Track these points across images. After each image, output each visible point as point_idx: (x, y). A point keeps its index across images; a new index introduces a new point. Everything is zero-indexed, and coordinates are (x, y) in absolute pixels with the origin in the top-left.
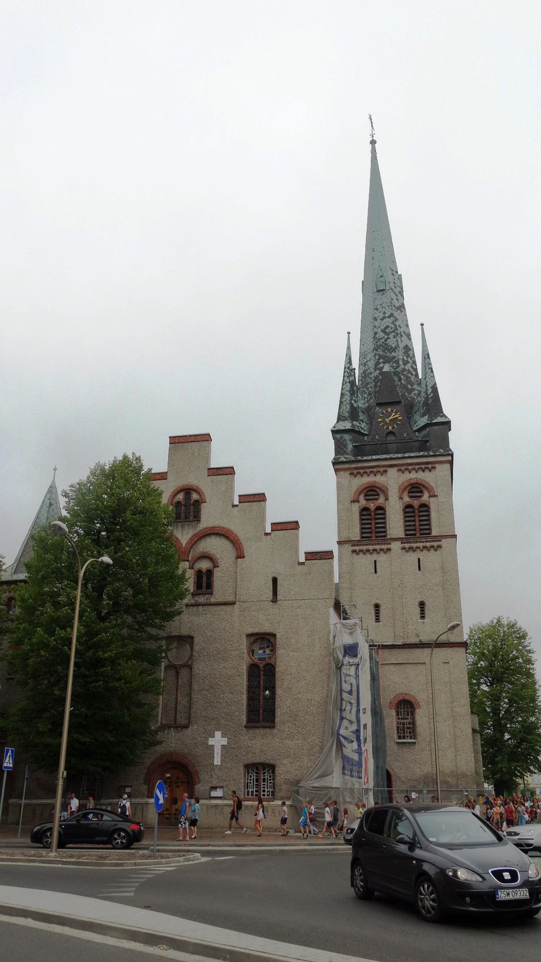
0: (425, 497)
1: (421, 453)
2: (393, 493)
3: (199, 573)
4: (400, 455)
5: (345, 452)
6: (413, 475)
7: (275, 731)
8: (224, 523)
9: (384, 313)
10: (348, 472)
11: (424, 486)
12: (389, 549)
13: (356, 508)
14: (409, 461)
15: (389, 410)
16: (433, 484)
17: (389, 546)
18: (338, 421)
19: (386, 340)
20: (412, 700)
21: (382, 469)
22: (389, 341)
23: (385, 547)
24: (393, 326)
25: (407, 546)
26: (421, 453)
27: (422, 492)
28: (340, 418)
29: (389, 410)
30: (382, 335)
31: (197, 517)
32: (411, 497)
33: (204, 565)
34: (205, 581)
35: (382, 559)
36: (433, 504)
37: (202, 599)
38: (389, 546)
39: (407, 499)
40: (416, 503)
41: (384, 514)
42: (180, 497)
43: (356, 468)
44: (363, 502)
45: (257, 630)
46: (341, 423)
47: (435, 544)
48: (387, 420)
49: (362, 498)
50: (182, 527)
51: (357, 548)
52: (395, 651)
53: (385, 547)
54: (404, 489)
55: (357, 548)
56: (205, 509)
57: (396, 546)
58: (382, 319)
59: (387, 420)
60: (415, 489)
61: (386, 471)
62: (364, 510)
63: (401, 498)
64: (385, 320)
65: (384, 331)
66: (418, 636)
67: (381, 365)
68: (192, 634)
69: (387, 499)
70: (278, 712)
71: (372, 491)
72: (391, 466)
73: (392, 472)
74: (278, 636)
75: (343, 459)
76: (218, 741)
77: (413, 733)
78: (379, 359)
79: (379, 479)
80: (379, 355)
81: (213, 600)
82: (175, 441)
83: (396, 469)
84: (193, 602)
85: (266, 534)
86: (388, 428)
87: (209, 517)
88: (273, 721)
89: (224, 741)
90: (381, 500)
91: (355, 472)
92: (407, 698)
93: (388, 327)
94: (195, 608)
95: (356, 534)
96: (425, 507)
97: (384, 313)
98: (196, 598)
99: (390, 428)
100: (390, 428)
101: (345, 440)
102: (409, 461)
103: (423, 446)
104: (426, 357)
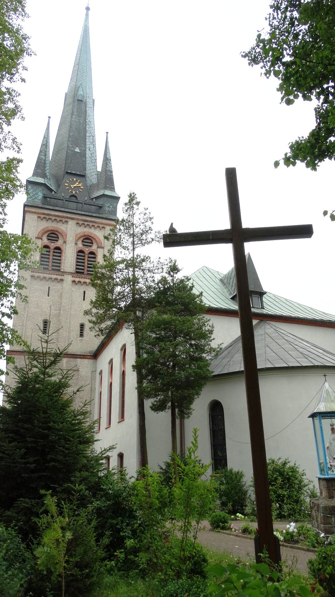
0: (94, 248)
11: (95, 239)
12: (62, 280)
15: (75, 179)
17: (62, 277)
18: (33, 176)
21: (64, 220)
23: (59, 277)
25: (77, 280)
29: (75, 179)
32: (84, 245)
35: (56, 287)
38: (62, 277)
39: (80, 245)
40: (87, 250)
41: (61, 253)
48: (72, 186)
51: (36, 275)
53: (59, 277)
54: (79, 238)
57: (69, 279)
59: (72, 186)
60: (88, 240)
63: (76, 244)
69: (65, 242)
71: (53, 235)
72: (73, 219)
73: (72, 223)
79: (61, 227)
83: (76, 222)
90: (59, 243)
91: (42, 216)
99: (74, 192)
100: (74, 192)
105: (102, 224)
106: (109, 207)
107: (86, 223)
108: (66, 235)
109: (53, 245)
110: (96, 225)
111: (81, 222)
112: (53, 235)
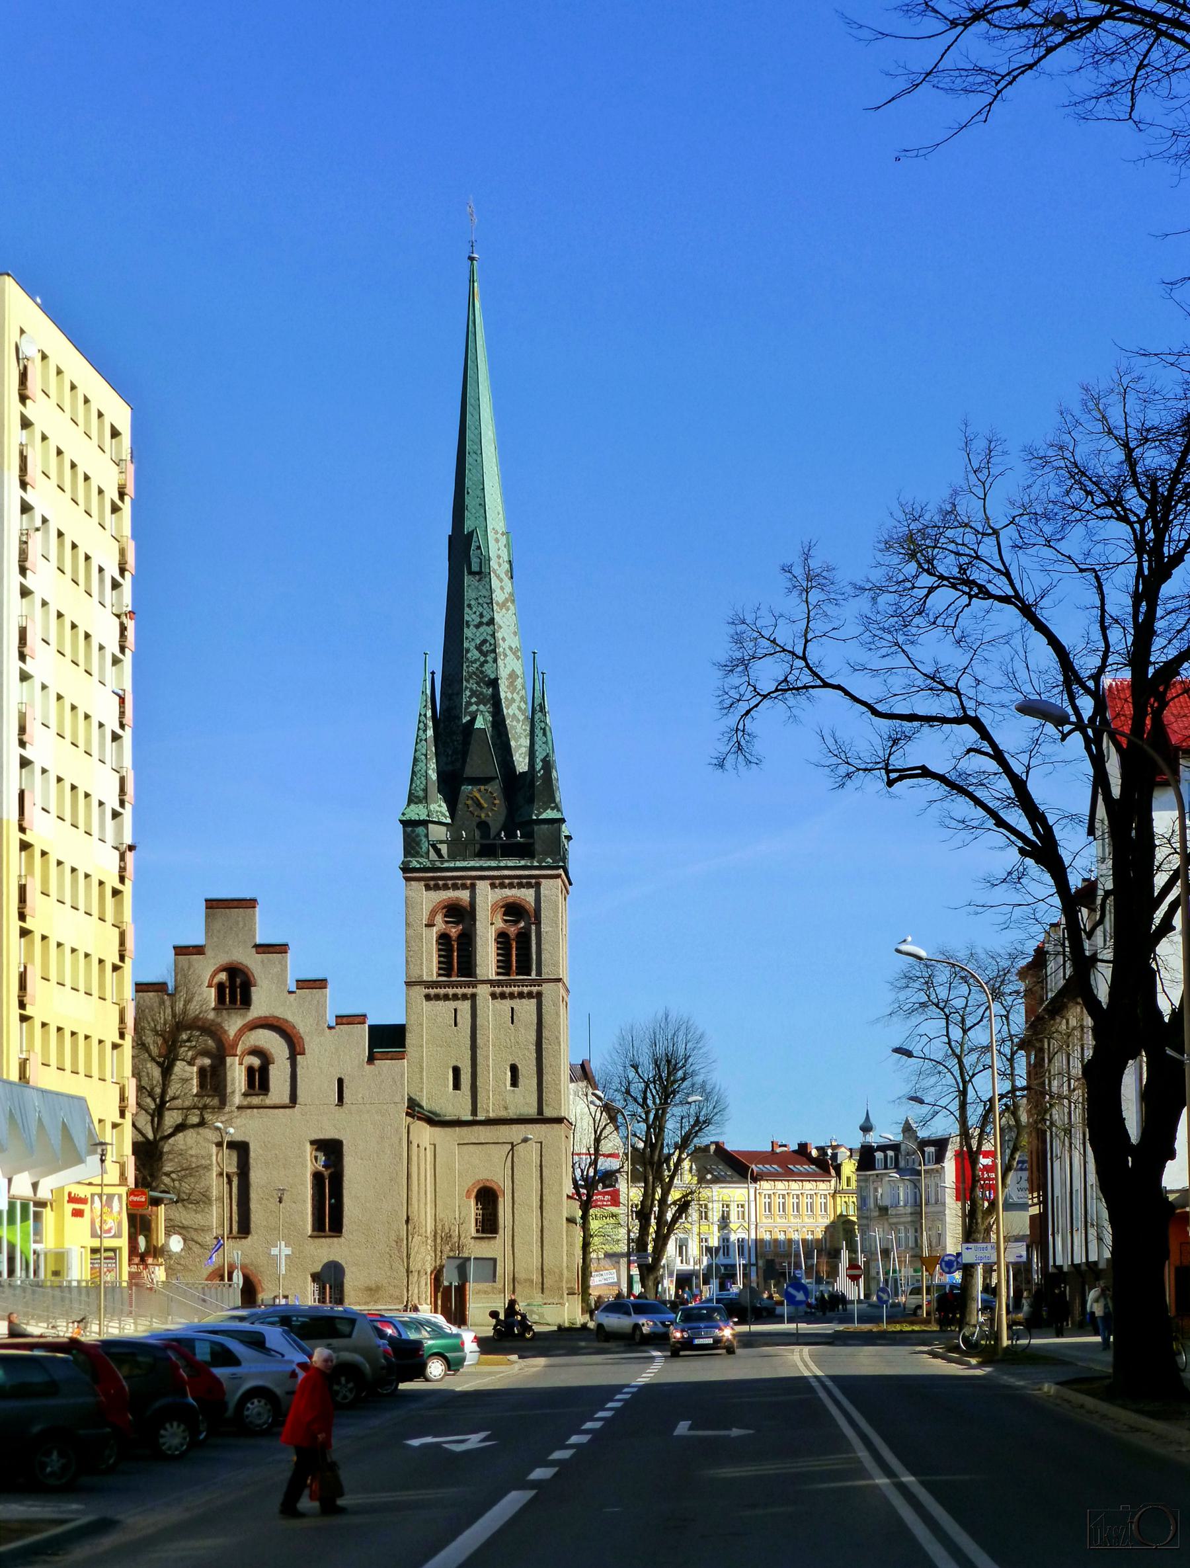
1: (523, 863)
3: (250, 1071)
4: (493, 864)
5: (418, 853)
6: (508, 892)
7: (342, 1240)
8: (278, 1013)
9: (481, 616)
10: (423, 883)
14: (506, 873)
18: (408, 805)
19: (482, 665)
20: (495, 1187)
22: (486, 666)
24: (492, 641)
25: (498, 990)
26: (523, 863)
28: (412, 799)
30: (476, 654)
31: (246, 1002)
32: (506, 921)
33: (256, 1062)
34: (258, 1080)
37: (256, 1100)
39: (500, 924)
42: (223, 976)
43: (433, 878)
45: (322, 1137)
46: (413, 806)
47: (535, 989)
49: (439, 919)
50: (229, 1014)
52: (476, 1128)
55: (432, 991)
56: (257, 994)
58: (477, 626)
60: (513, 910)
62: (443, 938)
64: (482, 629)
65: (479, 648)
66: (506, 1108)
67: (474, 708)
68: (247, 1139)
70: (346, 1221)
74: (345, 1142)
75: (415, 864)
76: (283, 1250)
77: (494, 1230)
78: (470, 697)
80: (471, 690)
81: (269, 1101)
82: (213, 905)
84: (245, 1103)
85: (330, 1028)
87: (261, 1006)
88: (341, 1231)
89: (288, 1251)
92: (488, 1184)
93: (485, 641)
94: (249, 1111)
95: (430, 968)
96: (524, 937)
97: (481, 616)
98: (249, 1099)
101: (418, 835)
102: (506, 873)
103: (524, 851)
104: (537, 710)
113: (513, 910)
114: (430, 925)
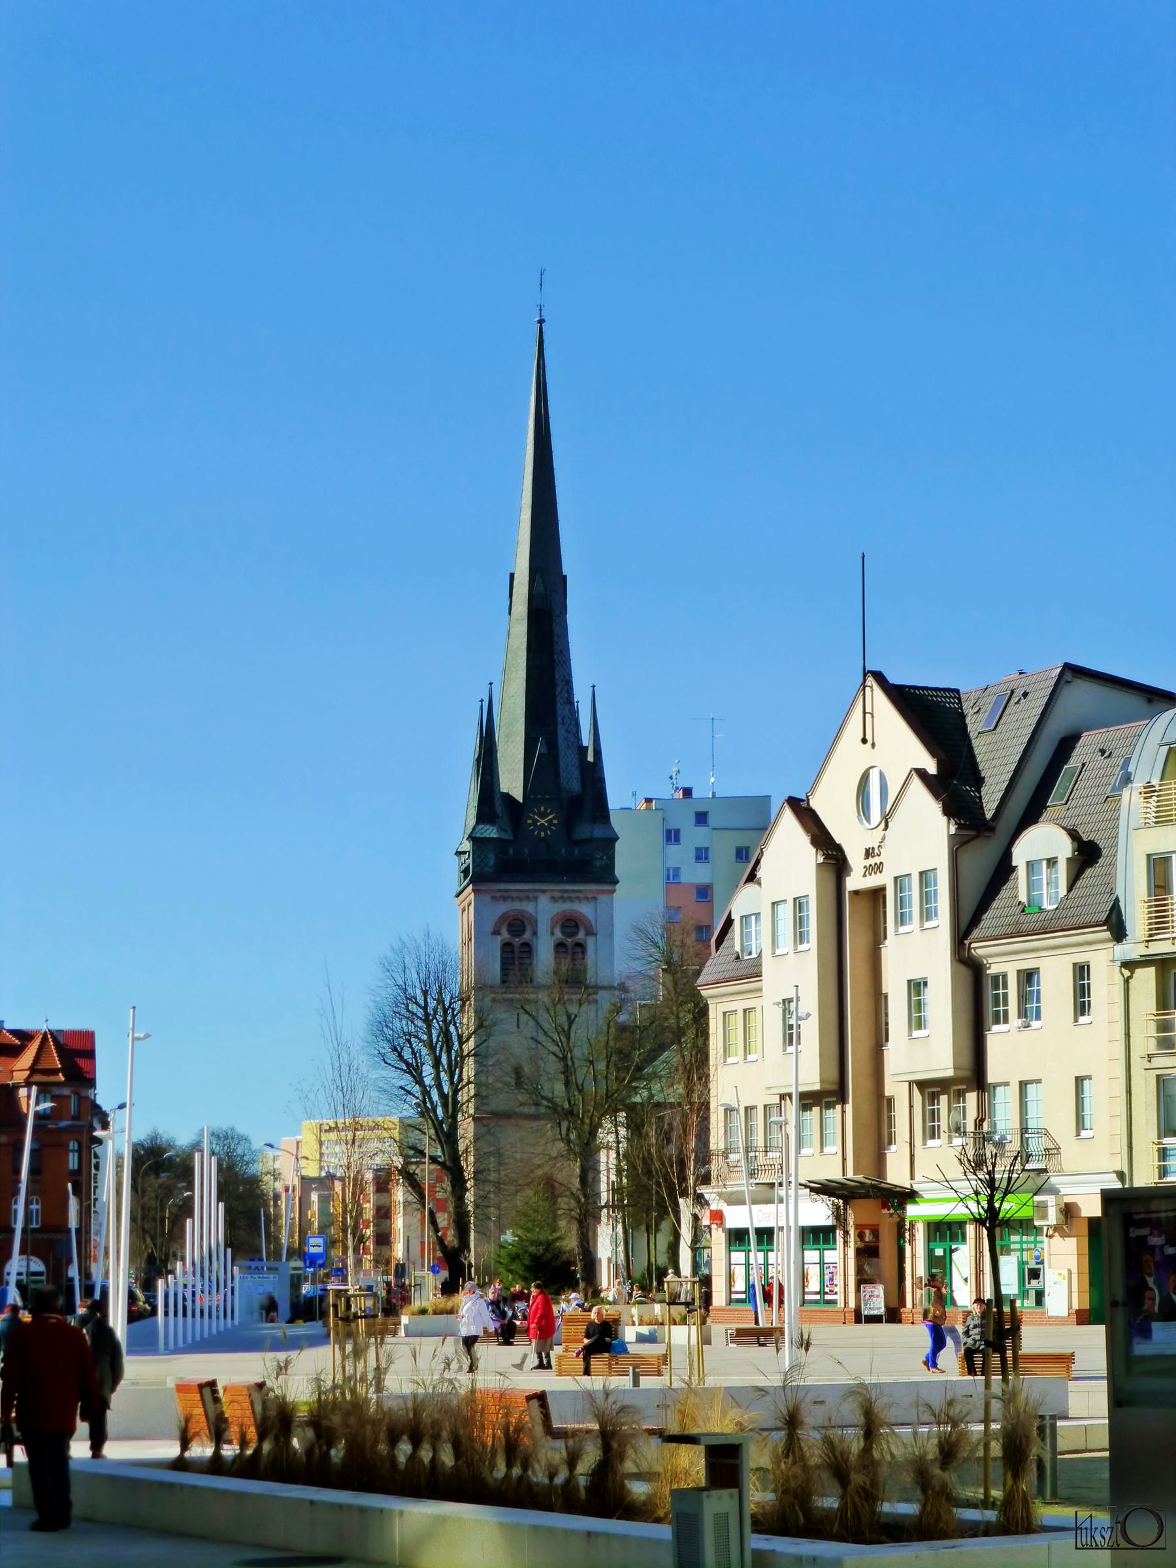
0: (581, 935)
2: (543, 927)
13: (498, 940)
16: (591, 917)
21: (531, 895)
27: (577, 926)
36: (590, 943)
39: (559, 934)
44: (505, 934)
46: (481, 826)
49: (504, 931)
60: (570, 924)
61: (536, 898)
62: (506, 946)
63: (552, 934)
69: (535, 933)
72: (544, 891)
79: (529, 907)
86: (539, 834)
90: (527, 936)
96: (581, 946)
99: (542, 834)
105: (591, 891)
106: (601, 859)
107: (566, 895)
108: (536, 922)
109: (517, 941)
110: (582, 895)
111: (557, 894)
112: (517, 924)
113: (570, 924)
114: (496, 932)
